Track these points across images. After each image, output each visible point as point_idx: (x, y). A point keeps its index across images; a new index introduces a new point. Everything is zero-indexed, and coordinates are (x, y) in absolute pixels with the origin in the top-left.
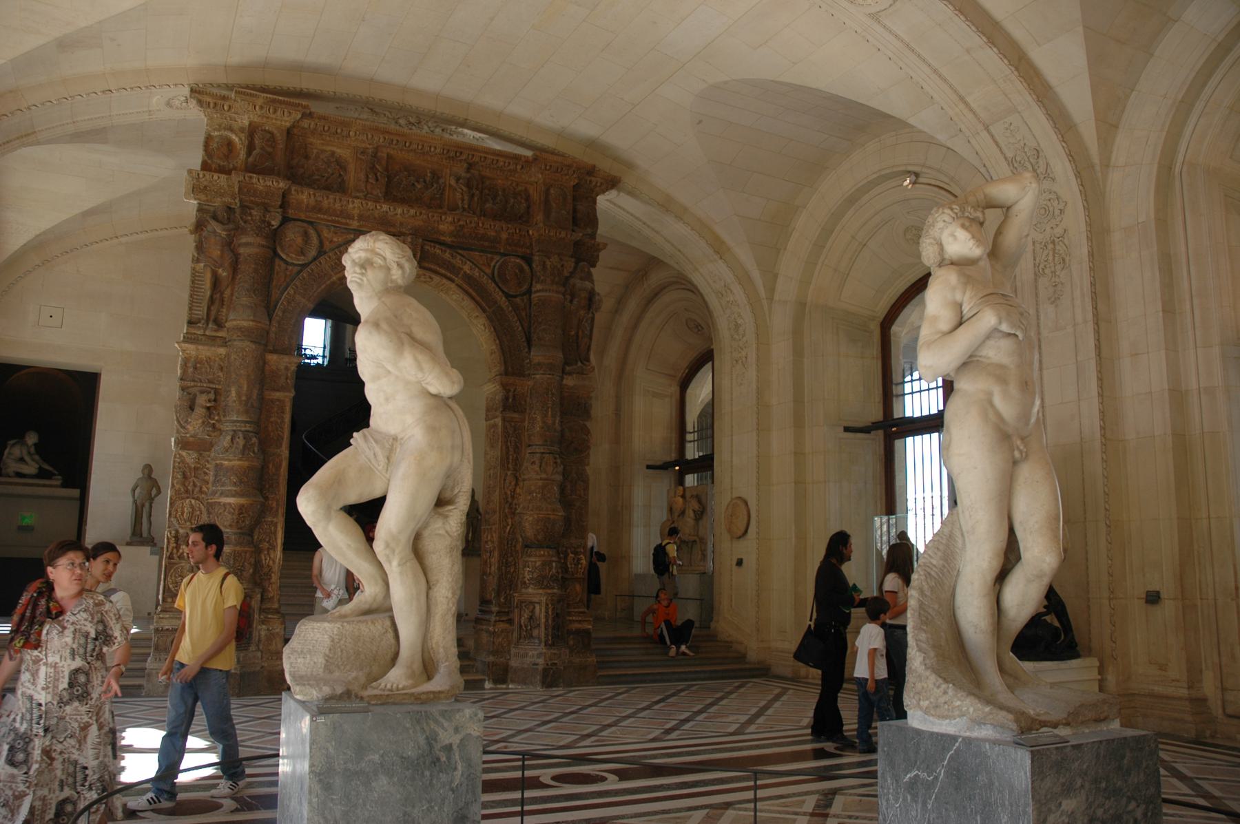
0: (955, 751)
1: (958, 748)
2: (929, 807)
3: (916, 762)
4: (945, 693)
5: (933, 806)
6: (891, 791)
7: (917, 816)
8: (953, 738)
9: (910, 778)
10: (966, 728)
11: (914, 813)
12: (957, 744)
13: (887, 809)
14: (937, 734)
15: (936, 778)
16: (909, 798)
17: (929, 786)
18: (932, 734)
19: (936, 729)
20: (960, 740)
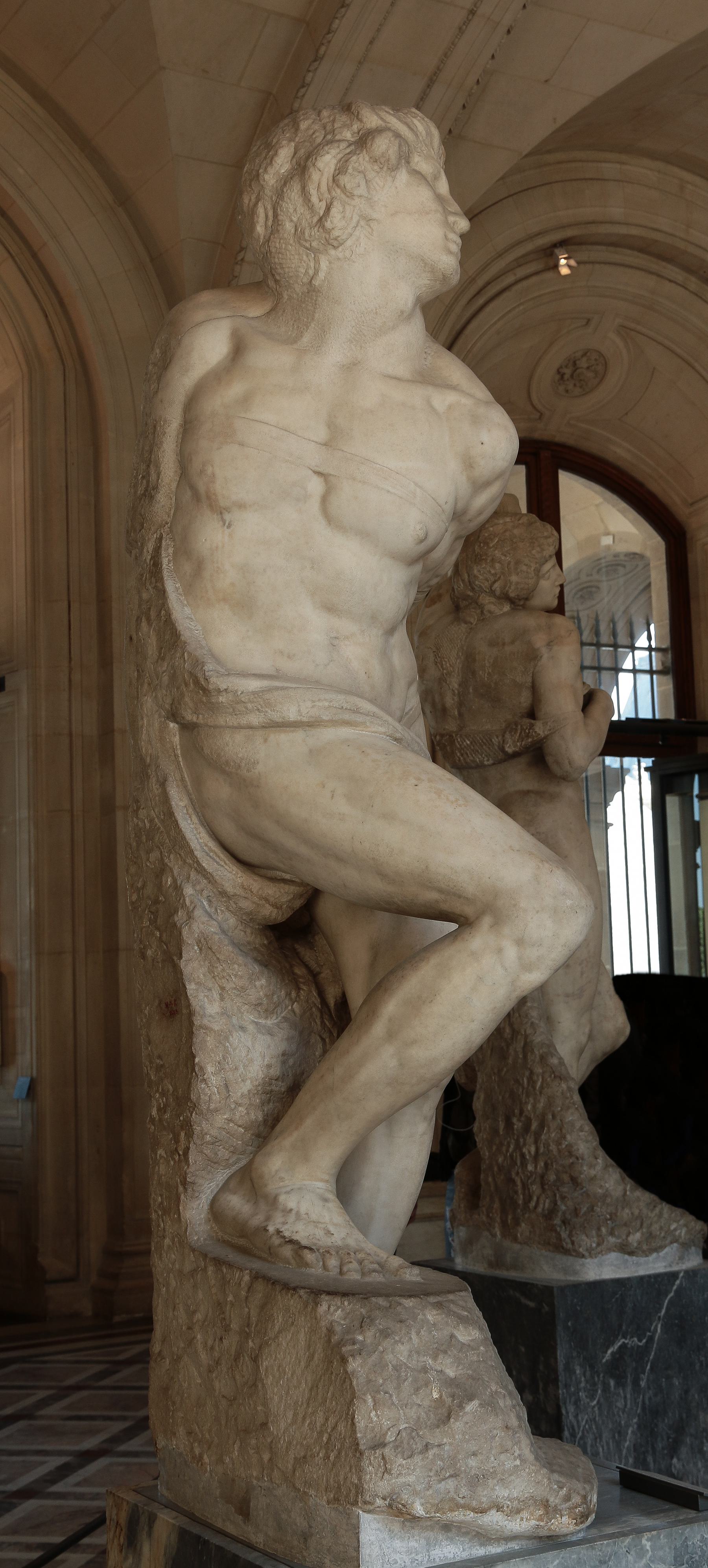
0: (676, 1291)
1: (680, 1287)
2: (643, 1384)
3: (620, 1326)
4: (660, 1215)
5: (648, 1380)
6: (583, 1385)
7: (626, 1405)
8: (672, 1276)
9: (613, 1354)
10: (677, 1258)
11: (620, 1404)
12: (678, 1282)
13: (576, 1416)
14: (649, 1276)
15: (651, 1339)
16: (612, 1383)
17: (641, 1354)
18: (641, 1278)
19: (642, 1272)
20: (681, 1275)
